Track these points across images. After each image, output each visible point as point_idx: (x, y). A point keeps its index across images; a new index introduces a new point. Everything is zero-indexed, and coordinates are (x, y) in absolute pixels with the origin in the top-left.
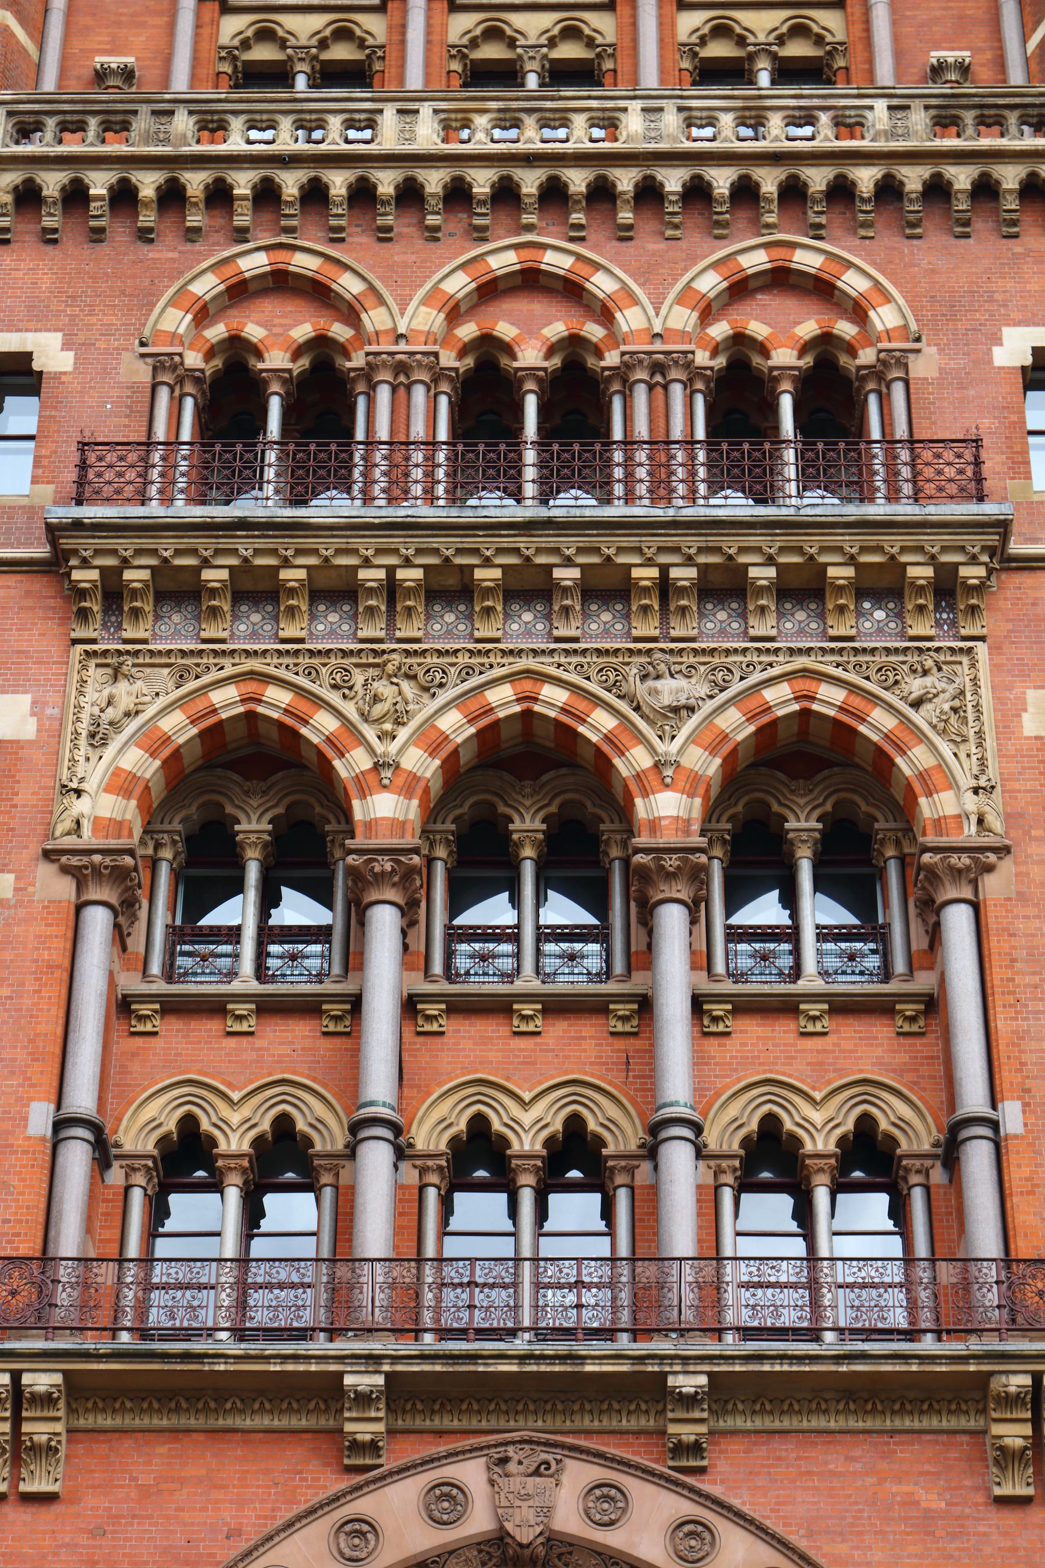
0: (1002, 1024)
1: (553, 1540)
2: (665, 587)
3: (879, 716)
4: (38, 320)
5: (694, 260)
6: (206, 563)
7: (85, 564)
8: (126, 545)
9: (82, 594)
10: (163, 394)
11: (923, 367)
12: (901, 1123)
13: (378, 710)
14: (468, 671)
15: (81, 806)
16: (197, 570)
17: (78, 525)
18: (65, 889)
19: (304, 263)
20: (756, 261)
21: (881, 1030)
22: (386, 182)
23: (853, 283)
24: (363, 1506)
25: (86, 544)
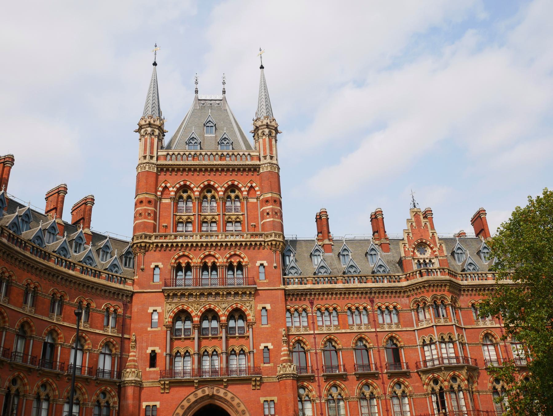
1: (213, 395)
2: (223, 294)
4: (159, 261)
5: (226, 253)
10: (172, 270)
11: (249, 266)
12: (245, 349)
13: (196, 308)
14: (204, 304)
15: (167, 320)
18: (165, 328)
20: (233, 253)
21: (244, 339)
24: (196, 392)
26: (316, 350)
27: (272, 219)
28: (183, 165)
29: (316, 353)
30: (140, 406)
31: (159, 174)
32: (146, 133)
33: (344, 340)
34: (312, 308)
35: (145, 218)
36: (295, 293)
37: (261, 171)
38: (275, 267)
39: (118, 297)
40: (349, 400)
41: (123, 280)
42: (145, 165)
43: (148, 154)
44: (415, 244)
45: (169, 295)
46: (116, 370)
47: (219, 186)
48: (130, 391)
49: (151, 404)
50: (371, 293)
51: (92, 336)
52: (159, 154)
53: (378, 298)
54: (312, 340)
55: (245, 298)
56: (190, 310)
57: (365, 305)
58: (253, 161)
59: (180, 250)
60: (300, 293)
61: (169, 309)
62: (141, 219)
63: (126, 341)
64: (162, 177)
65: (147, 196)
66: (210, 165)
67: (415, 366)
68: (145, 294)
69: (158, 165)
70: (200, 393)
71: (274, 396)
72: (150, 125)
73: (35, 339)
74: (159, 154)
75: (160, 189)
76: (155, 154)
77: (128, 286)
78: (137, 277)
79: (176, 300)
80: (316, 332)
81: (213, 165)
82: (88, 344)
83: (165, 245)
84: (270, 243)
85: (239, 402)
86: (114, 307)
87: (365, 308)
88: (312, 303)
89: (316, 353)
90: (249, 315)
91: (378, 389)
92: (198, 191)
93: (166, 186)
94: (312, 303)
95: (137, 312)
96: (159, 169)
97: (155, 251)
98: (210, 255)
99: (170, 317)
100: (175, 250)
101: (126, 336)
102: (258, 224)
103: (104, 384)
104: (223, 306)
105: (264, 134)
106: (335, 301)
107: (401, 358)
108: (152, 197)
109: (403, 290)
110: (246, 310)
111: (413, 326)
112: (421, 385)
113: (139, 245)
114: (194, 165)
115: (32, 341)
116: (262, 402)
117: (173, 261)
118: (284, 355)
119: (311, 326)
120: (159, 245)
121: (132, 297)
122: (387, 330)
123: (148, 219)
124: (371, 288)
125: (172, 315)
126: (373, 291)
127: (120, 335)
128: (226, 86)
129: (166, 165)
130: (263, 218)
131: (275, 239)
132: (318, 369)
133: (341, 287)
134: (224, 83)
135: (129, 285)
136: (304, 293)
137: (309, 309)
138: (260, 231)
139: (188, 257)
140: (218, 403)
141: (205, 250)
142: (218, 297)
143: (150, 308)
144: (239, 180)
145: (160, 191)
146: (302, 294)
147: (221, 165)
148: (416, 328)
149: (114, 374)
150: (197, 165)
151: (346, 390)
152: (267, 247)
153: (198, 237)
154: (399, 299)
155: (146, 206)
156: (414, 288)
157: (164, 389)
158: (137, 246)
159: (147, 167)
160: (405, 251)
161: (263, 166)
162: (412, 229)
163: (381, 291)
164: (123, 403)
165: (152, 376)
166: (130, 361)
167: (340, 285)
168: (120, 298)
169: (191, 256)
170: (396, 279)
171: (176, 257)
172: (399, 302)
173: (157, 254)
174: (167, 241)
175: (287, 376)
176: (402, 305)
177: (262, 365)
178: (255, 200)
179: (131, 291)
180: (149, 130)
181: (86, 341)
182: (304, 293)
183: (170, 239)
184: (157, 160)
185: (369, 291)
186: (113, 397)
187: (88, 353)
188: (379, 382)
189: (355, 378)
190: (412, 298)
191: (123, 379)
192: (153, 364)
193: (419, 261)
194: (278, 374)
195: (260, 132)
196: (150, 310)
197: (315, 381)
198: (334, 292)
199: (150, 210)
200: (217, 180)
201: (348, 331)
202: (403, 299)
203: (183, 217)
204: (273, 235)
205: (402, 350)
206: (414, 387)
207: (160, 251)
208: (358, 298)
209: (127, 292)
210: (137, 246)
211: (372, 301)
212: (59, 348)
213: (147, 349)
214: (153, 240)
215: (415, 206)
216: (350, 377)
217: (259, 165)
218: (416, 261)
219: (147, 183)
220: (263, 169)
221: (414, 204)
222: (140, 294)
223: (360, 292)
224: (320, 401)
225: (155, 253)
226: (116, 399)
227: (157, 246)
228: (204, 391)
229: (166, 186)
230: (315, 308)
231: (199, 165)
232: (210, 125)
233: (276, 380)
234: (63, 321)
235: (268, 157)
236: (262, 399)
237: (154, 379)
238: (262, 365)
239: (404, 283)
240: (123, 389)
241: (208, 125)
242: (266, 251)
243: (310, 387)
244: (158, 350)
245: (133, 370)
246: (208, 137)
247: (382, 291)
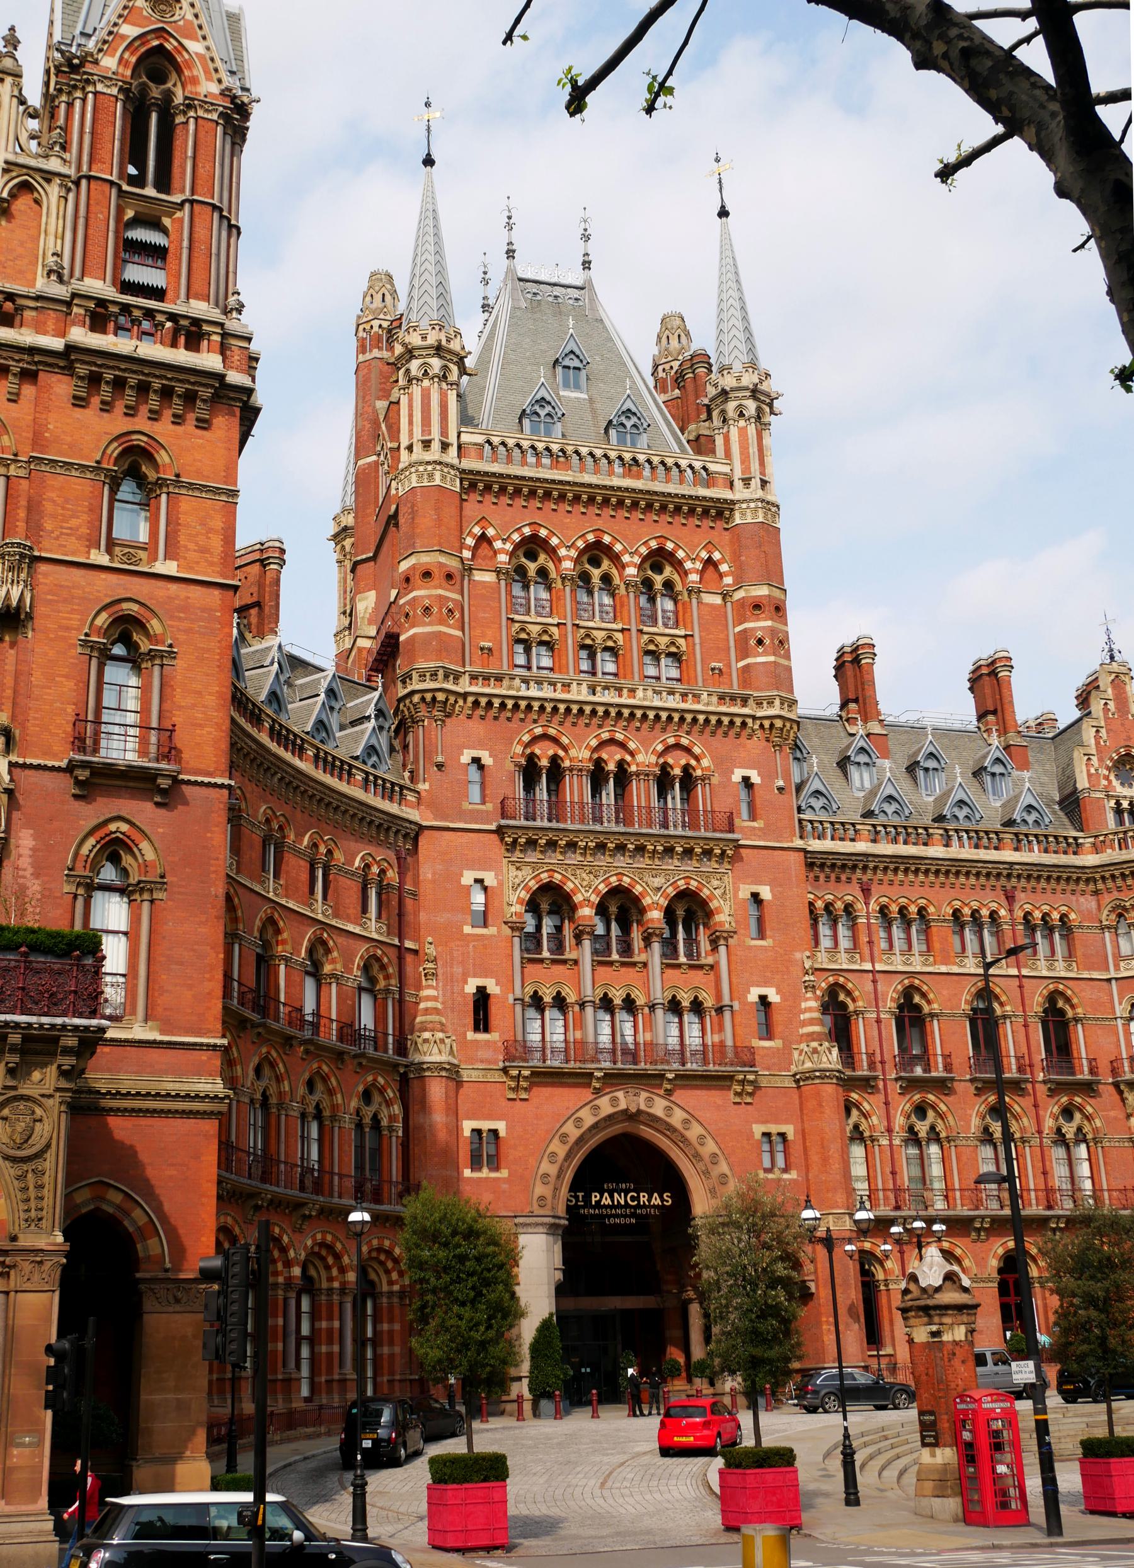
0: (734, 980)
3: (705, 890)
11: (715, 780)
18: (508, 932)
20: (671, 741)
21: (700, 973)
23: (697, 750)
24: (596, 1102)
25: (510, 832)
26: (878, 1012)
27: (772, 659)
28: (531, 479)
29: (878, 1021)
30: (458, 1129)
32: (426, 373)
33: (945, 992)
34: (867, 904)
35: (441, 622)
36: (829, 863)
37: (738, 521)
38: (780, 789)
39: (387, 837)
40: (958, 1142)
41: (392, 791)
42: (430, 468)
43: (435, 434)
44: (1111, 759)
46: (390, 1031)
48: (437, 1090)
49: (485, 1125)
50: (1009, 876)
51: (341, 940)
52: (465, 438)
53: (1024, 890)
54: (869, 987)
55: (711, 865)
56: (569, 886)
57: (994, 906)
58: (716, 490)
59: (535, 721)
60: (839, 863)
61: (517, 881)
62: (430, 624)
63: (409, 958)
64: (472, 508)
65: (443, 559)
66: (605, 487)
67: (1108, 1070)
69: (463, 471)
70: (605, 1106)
71: (787, 1122)
72: (439, 350)
74: (465, 438)
75: (470, 541)
76: (452, 439)
77: (409, 810)
78: (426, 786)
79: (533, 857)
80: (878, 967)
81: (612, 488)
82: (334, 961)
83: (496, 703)
84: (767, 723)
85: (704, 1132)
86: (378, 863)
87: (993, 915)
88: (866, 892)
89: (878, 1021)
90: (719, 910)
91: (1025, 1120)
92: (571, 559)
93: (483, 534)
94: (866, 892)
95: (434, 881)
96: (466, 483)
97: (469, 717)
98: (612, 741)
99: (520, 901)
100: (522, 720)
101: (409, 944)
102: (729, 666)
104: (657, 882)
105: (741, 415)
106: (923, 891)
107: (1074, 1047)
108: (453, 564)
109: (1084, 877)
110: (712, 897)
111: (1107, 969)
112: (1122, 1116)
113: (428, 696)
114: (561, 482)
116: (758, 1135)
117: (519, 749)
118: (811, 1022)
119: (866, 950)
120: (483, 701)
122: (1045, 973)
123: (449, 626)
124: (1012, 864)
125: (525, 895)
126: (1015, 873)
127: (396, 942)
128: (591, 247)
129: (486, 474)
130: (743, 653)
131: (783, 713)
132: (882, 1062)
133: (941, 856)
134: (586, 238)
136: (850, 863)
137: (860, 906)
138: (736, 689)
139: (555, 740)
140: (647, 1132)
141: (600, 726)
142: (619, 857)
143: (465, 873)
144: (678, 538)
145: (469, 548)
146: (844, 866)
147: (634, 490)
148: (1113, 974)
149: (386, 1043)
150: (568, 483)
151: (950, 1118)
152: (759, 733)
153: (584, 688)
154: (1074, 898)
155: (441, 587)
156: (1117, 873)
157: (515, 1089)
158: (423, 699)
159: (438, 476)
160: (1089, 775)
161: (744, 506)
162: (1106, 718)
163: (1034, 874)
164: (416, 1119)
165: (482, 1054)
166: (427, 1011)
167: (936, 851)
168: (391, 840)
169: (565, 740)
170: (1068, 844)
171: (526, 738)
172: (1074, 906)
173: (477, 727)
174: (504, 692)
175: (824, 1075)
176: (1079, 912)
177: (757, 1043)
178: (717, 600)
179: (416, 824)
180: (436, 363)
181: (328, 951)
182: (850, 863)
183: (510, 688)
185: (1005, 872)
186: (389, 1103)
187: (334, 986)
188: (1027, 1102)
189: (972, 1089)
190: (1107, 898)
191: (417, 1058)
192: (482, 1022)
193: (1118, 803)
194: (794, 1069)
195: (731, 406)
197: (878, 1091)
198: (923, 867)
200: (619, 533)
201: (956, 969)
202: (1082, 899)
203: (530, 627)
204: (777, 702)
205: (1079, 1026)
206: (1107, 1121)
207: (482, 718)
208: (978, 888)
210: (423, 699)
211: (1010, 898)
212: (282, 967)
213: (466, 982)
214: (464, 685)
215: (1112, 658)
216: (959, 1087)
217: (733, 502)
218: (1112, 803)
219: (439, 521)
220: (743, 514)
221: (1111, 650)
223: (984, 871)
224: (890, 1140)
225: (470, 723)
226: (397, 1109)
227: (476, 704)
228: (614, 1101)
229: (483, 534)
230: (874, 906)
231: (575, 484)
232: (572, 364)
233: (790, 1083)
234: (287, 896)
235: (755, 483)
236: (758, 1129)
237: (489, 1062)
238: (757, 1043)
239: (1090, 859)
240: (415, 1086)
241: (567, 362)
242: (756, 745)
243: (865, 1105)
244: (493, 988)
245: (440, 1035)
246: (569, 399)
247: (1035, 874)
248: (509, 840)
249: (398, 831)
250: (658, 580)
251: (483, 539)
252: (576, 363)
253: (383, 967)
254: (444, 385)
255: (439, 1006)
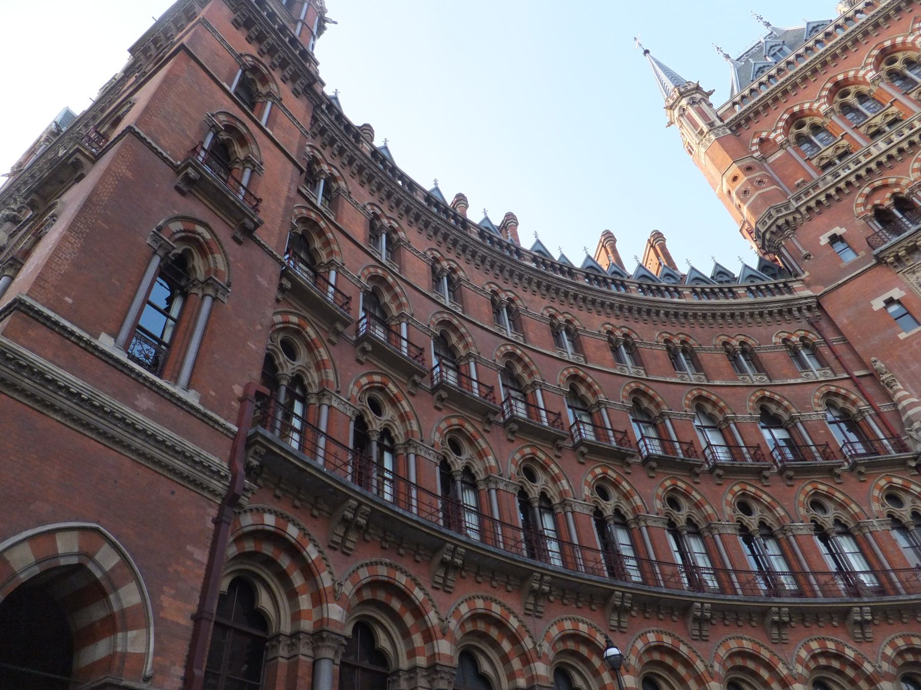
6: (916, 241)
7: (888, 257)
8: (895, 249)
9: (892, 263)
16: (915, 245)
17: (882, 251)
19: (878, 183)
22: (883, 159)
31: (738, 134)
45: (898, 259)
46: (882, 436)
47: (858, 71)
62: (751, 197)
64: (746, 133)
68: (844, 287)
73: (671, 417)
77: (799, 293)
78: (807, 274)
93: (761, 139)
96: (734, 128)
103: (880, 474)
115: (668, 422)
121: (819, 306)
127: (846, 376)
135: (800, 289)
158: (772, 233)
169: (892, 180)
173: (819, 221)
179: (811, 297)
184: (722, 120)
196: (878, 304)
199: (757, 176)
209: (805, 301)
222: (833, 295)
225: (814, 222)
248: (891, 259)
249: (800, 310)
250: (898, 65)
251: (762, 141)
252: (778, 48)
253: (845, 398)
254: (696, 106)
255: (915, 400)
